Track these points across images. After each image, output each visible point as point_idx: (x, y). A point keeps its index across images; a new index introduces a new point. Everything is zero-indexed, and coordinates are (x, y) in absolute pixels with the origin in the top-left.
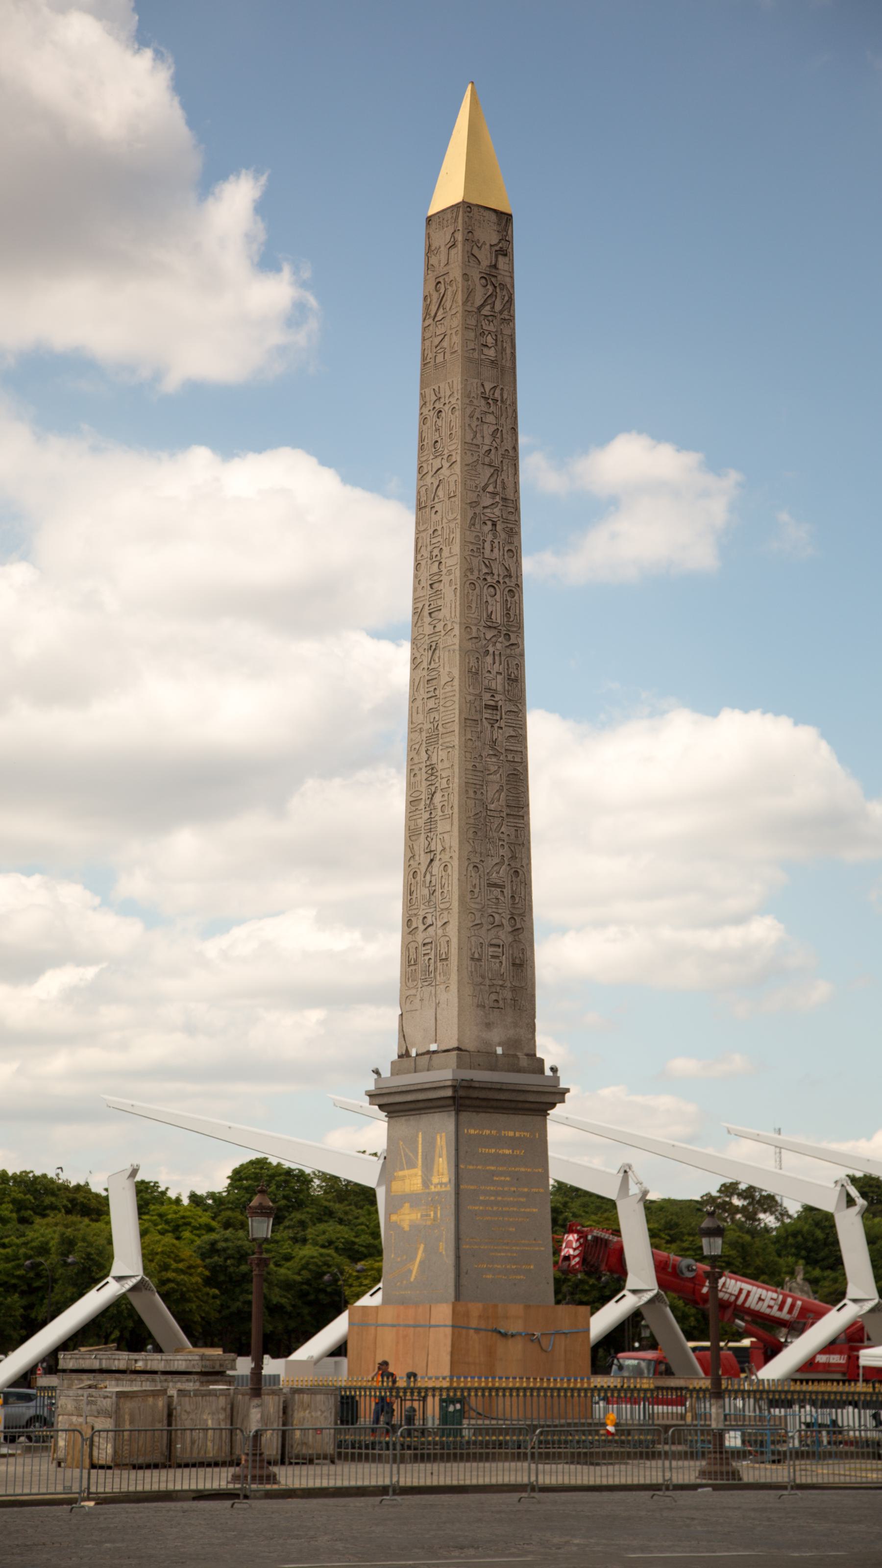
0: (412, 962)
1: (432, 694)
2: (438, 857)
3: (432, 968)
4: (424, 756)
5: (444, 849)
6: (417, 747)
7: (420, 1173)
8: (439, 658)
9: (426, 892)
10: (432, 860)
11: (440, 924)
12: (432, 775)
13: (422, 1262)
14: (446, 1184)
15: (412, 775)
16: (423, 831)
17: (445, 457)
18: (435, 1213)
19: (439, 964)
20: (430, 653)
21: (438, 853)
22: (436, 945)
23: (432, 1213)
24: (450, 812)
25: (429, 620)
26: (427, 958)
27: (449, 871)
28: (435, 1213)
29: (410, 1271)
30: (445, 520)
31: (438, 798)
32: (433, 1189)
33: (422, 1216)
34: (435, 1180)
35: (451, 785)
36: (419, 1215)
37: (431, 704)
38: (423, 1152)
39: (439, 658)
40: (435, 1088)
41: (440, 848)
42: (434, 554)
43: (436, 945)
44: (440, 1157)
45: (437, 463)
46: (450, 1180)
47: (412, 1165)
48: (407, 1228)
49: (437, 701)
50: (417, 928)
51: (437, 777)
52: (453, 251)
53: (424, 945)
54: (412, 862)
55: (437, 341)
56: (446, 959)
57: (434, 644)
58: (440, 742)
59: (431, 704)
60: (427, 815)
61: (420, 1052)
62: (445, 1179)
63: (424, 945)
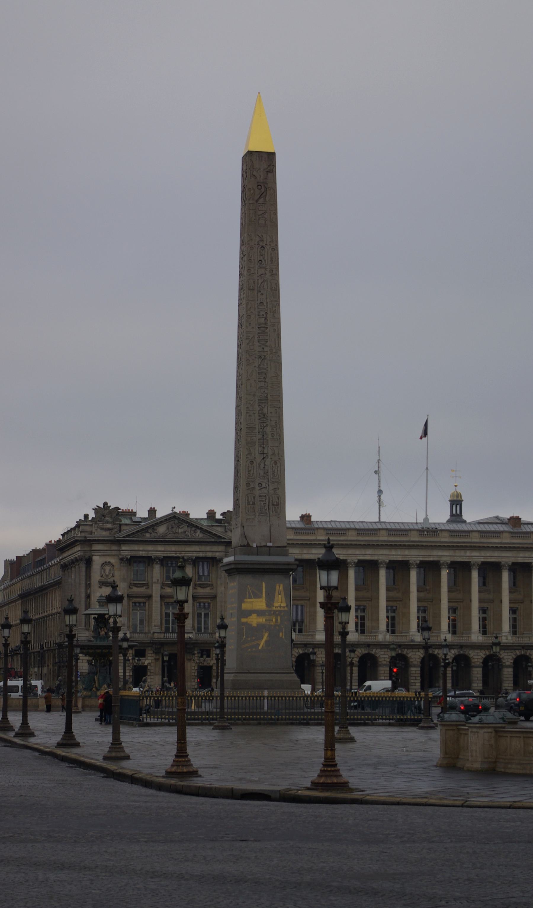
0: (251, 503)
1: (263, 380)
2: (269, 457)
3: (266, 507)
4: (257, 408)
5: (274, 454)
6: (251, 402)
7: (264, 601)
8: (267, 364)
9: (262, 472)
10: (264, 458)
11: (271, 488)
12: (263, 418)
13: (266, 641)
14: (284, 607)
15: (248, 415)
16: (257, 443)
17: (268, 270)
18: (277, 620)
19: (271, 506)
20: (260, 361)
21: (269, 455)
22: (269, 498)
23: (274, 620)
24: (278, 438)
25: (258, 344)
26: (263, 503)
27: (278, 465)
28: (277, 620)
29: (259, 645)
30: (268, 300)
31: (268, 430)
32: (274, 608)
33: (266, 620)
34: (276, 604)
35: (278, 425)
36: (264, 620)
37: (262, 384)
38: (266, 592)
39: (267, 364)
40: (280, 564)
41: (270, 453)
42: (261, 313)
43: (269, 498)
44: (279, 594)
45: (263, 271)
46: (287, 606)
47: (258, 596)
48: (255, 625)
49: (266, 384)
50: (254, 488)
51: (267, 419)
52: (270, 175)
53: (260, 496)
54: (249, 456)
55: (260, 213)
56: (277, 505)
57: (263, 357)
58: (269, 403)
59: (262, 384)
60: (260, 436)
61: (258, 545)
62: (284, 605)
63: (260, 496)
